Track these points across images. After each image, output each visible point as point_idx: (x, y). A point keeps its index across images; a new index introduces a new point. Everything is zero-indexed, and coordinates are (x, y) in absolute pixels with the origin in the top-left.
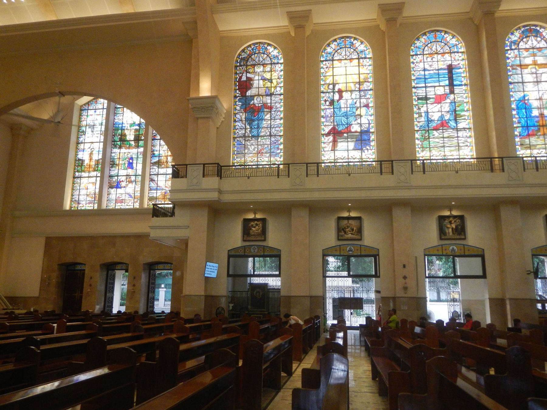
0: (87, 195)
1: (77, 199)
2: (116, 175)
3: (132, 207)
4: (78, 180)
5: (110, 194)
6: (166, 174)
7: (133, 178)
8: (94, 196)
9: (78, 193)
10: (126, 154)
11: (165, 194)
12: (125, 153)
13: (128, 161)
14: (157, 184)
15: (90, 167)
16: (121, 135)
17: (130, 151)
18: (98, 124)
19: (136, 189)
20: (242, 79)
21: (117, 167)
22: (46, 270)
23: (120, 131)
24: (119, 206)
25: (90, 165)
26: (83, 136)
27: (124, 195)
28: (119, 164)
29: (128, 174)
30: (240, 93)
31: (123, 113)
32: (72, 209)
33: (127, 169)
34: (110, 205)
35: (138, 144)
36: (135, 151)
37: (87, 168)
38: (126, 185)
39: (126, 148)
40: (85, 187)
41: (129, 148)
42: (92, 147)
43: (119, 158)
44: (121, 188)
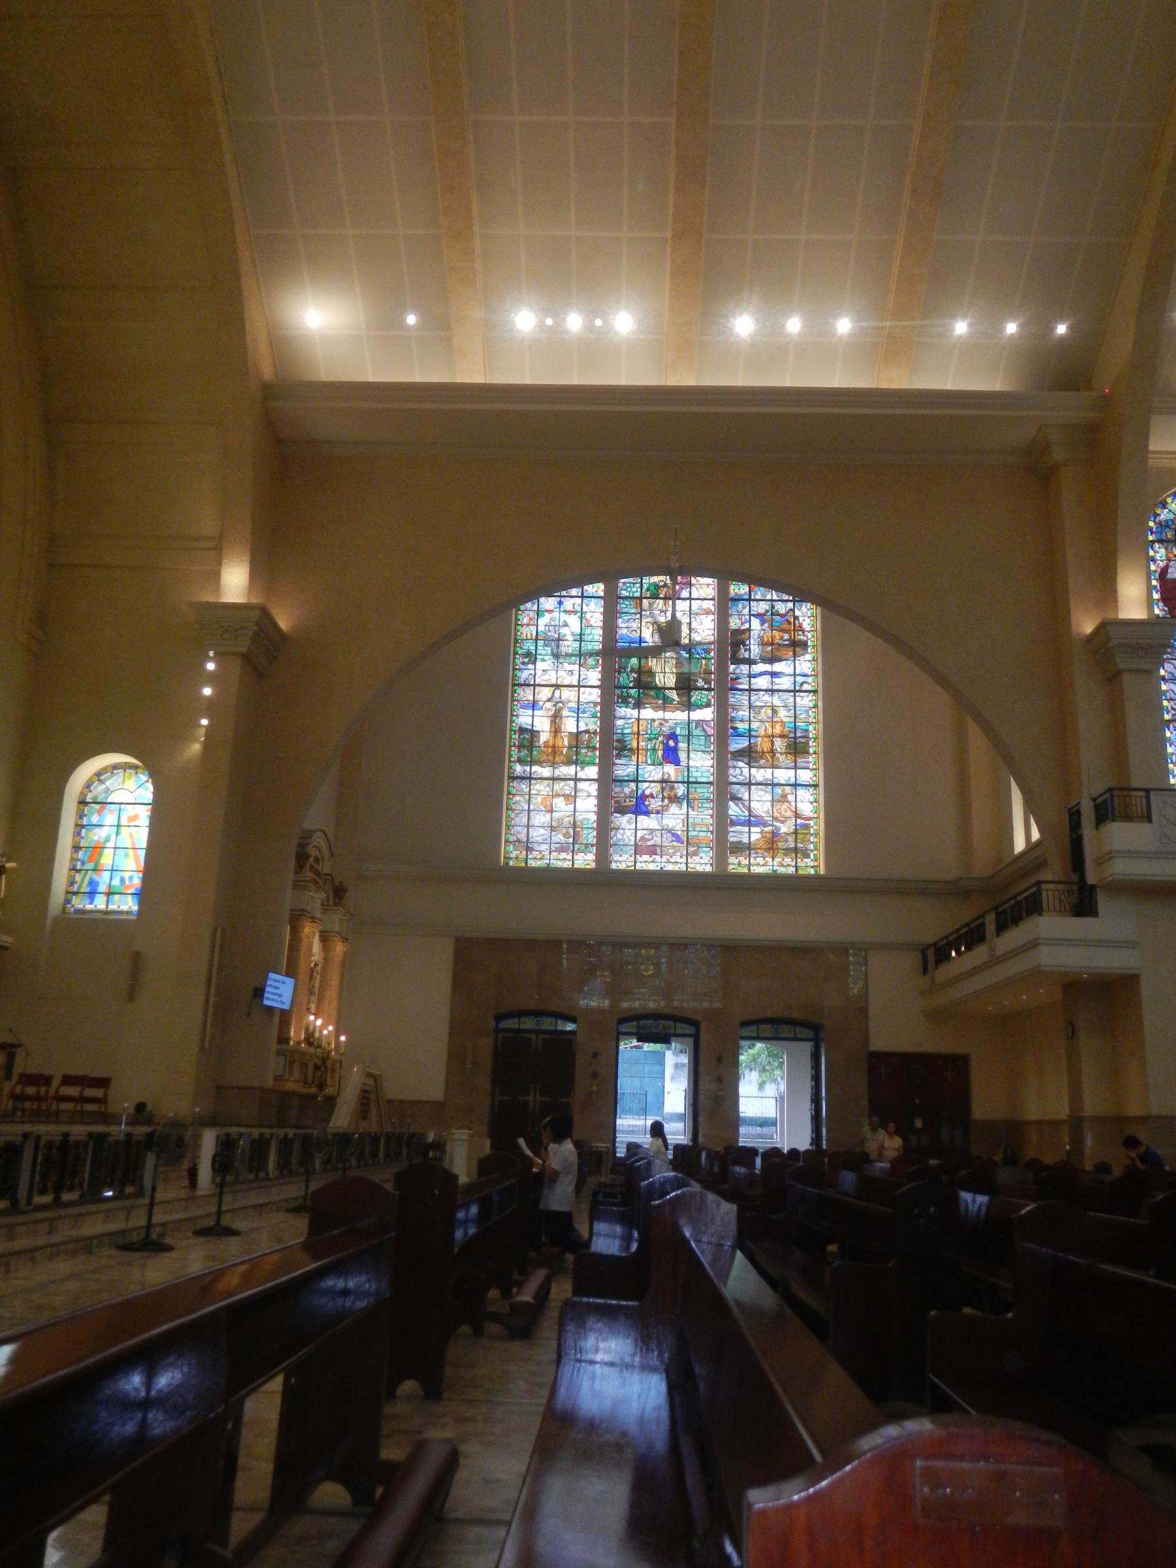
1: (523, 837)
3: (683, 867)
4: (523, 786)
5: (619, 829)
6: (773, 785)
7: (681, 790)
8: (571, 831)
9: (525, 821)
10: (657, 723)
11: (773, 836)
12: (653, 720)
13: (662, 742)
14: (750, 811)
15: (554, 753)
16: (639, 671)
17: (669, 715)
19: (690, 820)
20: (1169, 576)
21: (634, 758)
22: (459, 1028)
24: (647, 863)
25: (554, 747)
26: (530, 666)
27: (659, 833)
28: (638, 749)
29: (666, 777)
30: (1166, 609)
31: (641, 614)
32: (511, 863)
33: (661, 764)
34: (620, 859)
35: (689, 700)
36: (681, 716)
37: (548, 755)
38: (662, 806)
39: (656, 709)
40: (545, 807)
41: (664, 709)
43: (638, 734)
44: (647, 813)
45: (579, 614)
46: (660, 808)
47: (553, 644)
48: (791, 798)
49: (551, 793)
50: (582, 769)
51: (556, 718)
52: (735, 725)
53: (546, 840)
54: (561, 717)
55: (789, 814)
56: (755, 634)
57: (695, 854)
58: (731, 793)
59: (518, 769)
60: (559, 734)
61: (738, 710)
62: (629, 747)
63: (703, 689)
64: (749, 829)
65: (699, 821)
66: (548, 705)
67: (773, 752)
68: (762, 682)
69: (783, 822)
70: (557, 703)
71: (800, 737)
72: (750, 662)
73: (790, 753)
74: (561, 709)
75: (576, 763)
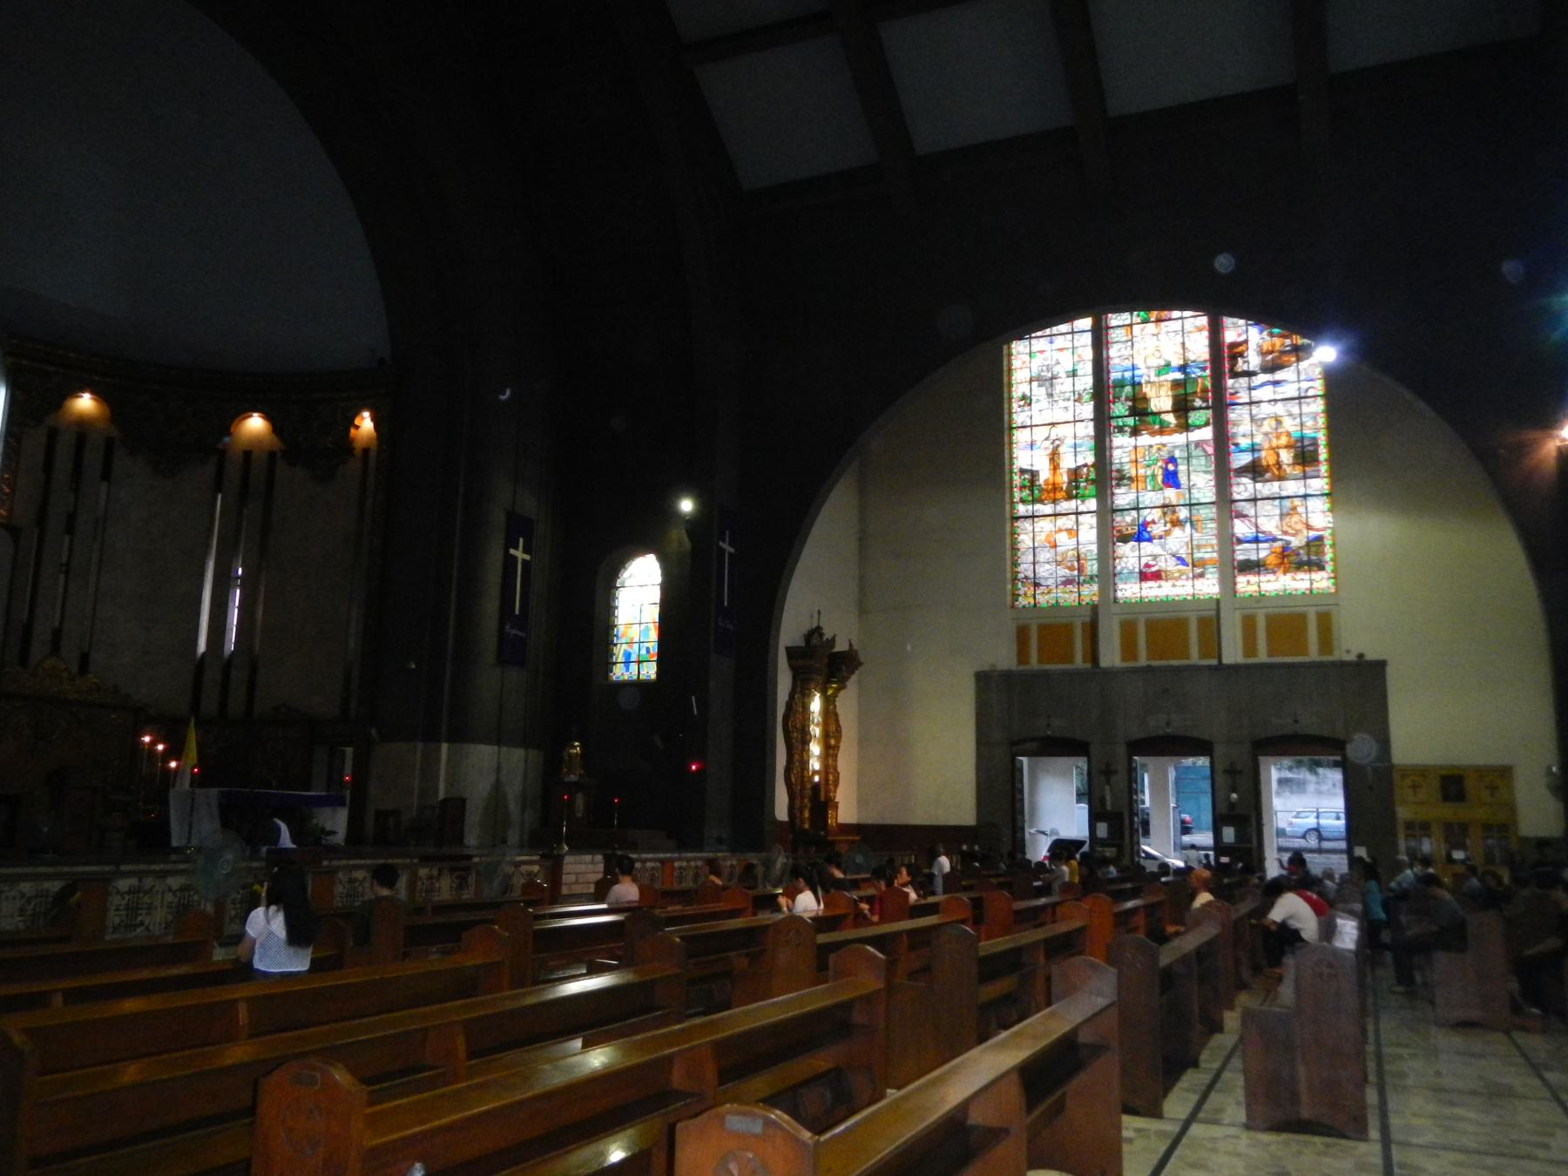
0: (1056, 561)
2: (1132, 506)
6: (1281, 498)
7: (1183, 513)
8: (1076, 564)
9: (1031, 558)
10: (1154, 449)
12: (1151, 446)
13: (1161, 467)
14: (1257, 527)
17: (1165, 439)
18: (1063, 375)
19: (1195, 543)
23: (1128, 389)
25: (1054, 484)
29: (1167, 502)
31: (1132, 340)
33: (1161, 489)
35: (1187, 421)
36: (1179, 438)
37: (1048, 492)
38: (1166, 531)
39: (1153, 434)
40: (1049, 543)
42: (1053, 437)
44: (1150, 540)
45: (1071, 350)
46: (1163, 533)
47: (1047, 384)
48: (1300, 510)
49: (1053, 529)
50: (1083, 502)
51: (1054, 457)
52: (1236, 441)
53: (1052, 574)
54: (1059, 454)
55: (1299, 526)
56: (1252, 345)
57: (1202, 575)
58: (1236, 512)
59: (1022, 509)
60: (1058, 471)
61: (1238, 425)
62: (1128, 475)
63: (1201, 408)
64: (1258, 546)
65: (1203, 542)
66: (1047, 443)
67: (1279, 464)
68: (1265, 393)
69: (1293, 535)
70: (1054, 441)
71: (1308, 446)
72: (1249, 374)
73: (1298, 464)
74: (1058, 446)
75: (1076, 497)
